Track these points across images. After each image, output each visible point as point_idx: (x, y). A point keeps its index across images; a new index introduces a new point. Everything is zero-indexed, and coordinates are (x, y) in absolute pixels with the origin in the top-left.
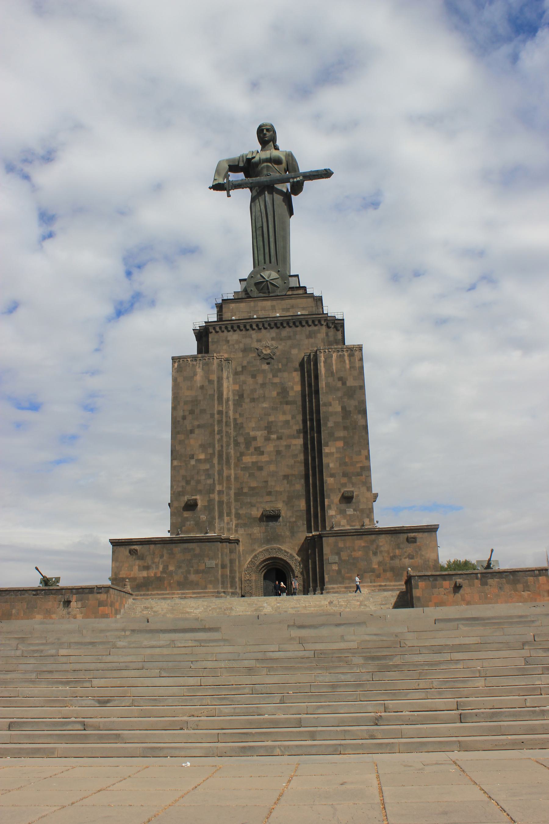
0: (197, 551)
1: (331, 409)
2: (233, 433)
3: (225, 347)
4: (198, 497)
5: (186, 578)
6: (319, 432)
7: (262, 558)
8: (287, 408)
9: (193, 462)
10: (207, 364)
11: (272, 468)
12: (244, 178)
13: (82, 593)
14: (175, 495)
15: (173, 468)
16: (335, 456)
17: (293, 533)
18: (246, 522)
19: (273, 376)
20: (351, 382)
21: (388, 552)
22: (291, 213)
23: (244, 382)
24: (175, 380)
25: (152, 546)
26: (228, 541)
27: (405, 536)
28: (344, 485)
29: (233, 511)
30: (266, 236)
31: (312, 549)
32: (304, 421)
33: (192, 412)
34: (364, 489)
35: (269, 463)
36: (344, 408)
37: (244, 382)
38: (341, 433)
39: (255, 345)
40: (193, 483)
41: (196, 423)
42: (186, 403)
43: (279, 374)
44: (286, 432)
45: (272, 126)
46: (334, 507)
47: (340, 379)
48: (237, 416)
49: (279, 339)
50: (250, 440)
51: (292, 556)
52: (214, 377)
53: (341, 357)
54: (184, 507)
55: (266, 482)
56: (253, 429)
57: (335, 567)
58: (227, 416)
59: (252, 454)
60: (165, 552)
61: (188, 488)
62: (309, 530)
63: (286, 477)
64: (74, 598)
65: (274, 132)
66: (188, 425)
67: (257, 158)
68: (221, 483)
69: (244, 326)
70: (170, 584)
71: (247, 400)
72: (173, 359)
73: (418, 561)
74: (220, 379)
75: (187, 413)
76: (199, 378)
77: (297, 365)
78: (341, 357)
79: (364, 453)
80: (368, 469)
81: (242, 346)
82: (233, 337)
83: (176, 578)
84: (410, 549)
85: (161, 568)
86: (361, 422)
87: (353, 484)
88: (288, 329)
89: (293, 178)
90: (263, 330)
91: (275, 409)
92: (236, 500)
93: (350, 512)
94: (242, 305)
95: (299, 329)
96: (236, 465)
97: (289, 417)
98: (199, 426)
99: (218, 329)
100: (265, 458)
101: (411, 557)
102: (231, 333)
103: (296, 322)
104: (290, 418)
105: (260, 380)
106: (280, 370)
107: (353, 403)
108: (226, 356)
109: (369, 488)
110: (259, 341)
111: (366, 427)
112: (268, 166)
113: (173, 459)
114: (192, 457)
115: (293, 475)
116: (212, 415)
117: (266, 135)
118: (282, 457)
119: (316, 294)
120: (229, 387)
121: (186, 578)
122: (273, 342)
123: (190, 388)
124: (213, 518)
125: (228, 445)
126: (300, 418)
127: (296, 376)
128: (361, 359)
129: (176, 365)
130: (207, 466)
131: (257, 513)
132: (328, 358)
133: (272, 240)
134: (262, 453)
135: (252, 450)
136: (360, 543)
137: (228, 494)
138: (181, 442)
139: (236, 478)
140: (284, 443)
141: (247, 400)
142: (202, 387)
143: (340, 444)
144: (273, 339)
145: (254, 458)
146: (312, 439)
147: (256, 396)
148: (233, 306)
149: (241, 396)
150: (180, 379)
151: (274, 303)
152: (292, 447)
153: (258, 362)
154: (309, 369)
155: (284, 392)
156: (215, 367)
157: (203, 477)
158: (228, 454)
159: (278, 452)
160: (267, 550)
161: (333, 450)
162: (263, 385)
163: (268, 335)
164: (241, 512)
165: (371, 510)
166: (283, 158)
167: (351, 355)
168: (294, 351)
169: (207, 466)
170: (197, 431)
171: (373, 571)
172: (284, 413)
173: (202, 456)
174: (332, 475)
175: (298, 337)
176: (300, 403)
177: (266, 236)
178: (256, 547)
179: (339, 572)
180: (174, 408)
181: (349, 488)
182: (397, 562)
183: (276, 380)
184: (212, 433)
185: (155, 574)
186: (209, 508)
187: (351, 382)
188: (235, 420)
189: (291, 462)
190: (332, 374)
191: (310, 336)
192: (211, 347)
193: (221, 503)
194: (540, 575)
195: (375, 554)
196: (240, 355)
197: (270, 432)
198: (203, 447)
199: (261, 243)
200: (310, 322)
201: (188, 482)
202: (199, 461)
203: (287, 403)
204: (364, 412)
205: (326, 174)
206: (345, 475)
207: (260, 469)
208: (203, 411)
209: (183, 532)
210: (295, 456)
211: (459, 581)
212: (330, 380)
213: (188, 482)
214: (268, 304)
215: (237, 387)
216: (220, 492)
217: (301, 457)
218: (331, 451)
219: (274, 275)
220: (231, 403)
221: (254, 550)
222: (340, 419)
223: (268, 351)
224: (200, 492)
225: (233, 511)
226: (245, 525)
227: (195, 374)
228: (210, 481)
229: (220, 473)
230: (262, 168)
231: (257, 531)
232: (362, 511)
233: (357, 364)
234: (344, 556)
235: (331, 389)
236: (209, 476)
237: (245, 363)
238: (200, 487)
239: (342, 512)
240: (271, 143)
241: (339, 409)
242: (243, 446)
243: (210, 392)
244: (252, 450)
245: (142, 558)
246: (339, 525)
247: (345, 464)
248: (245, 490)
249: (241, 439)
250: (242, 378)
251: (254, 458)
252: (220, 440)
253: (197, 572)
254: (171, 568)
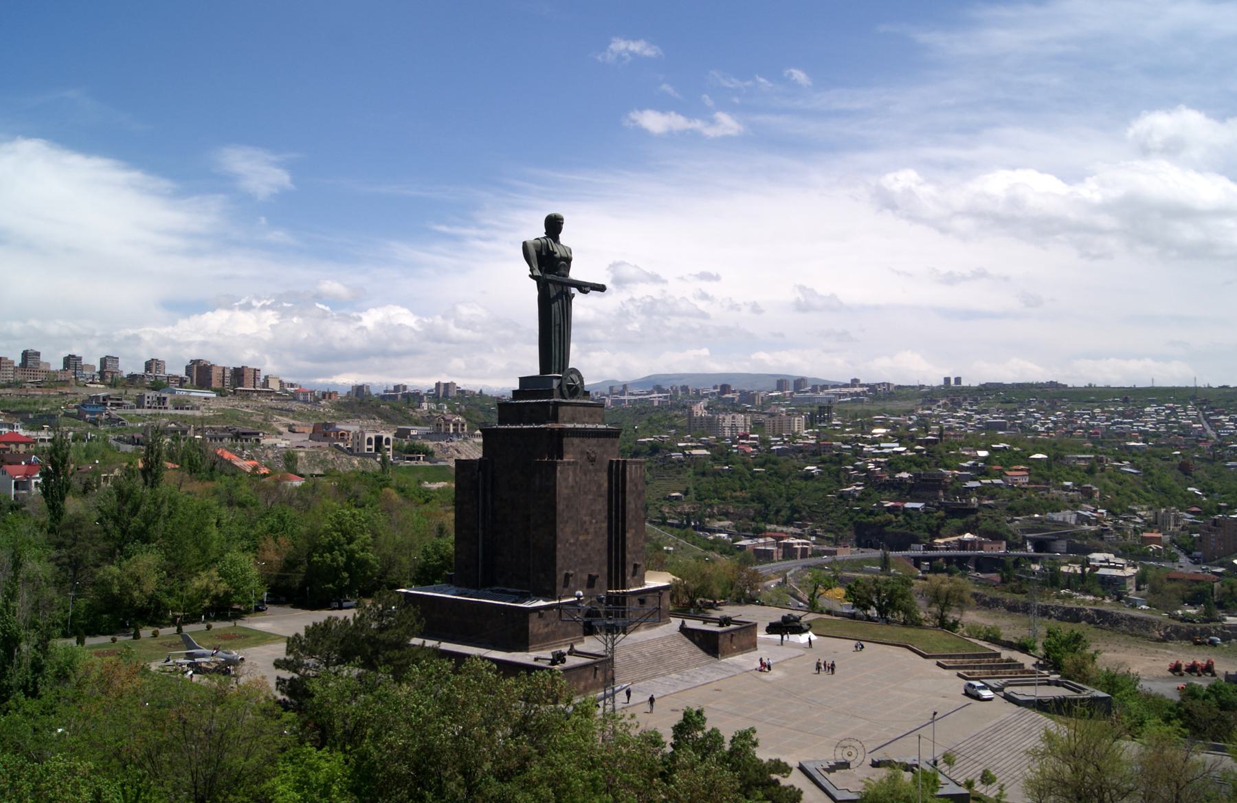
8: (600, 499)
32: (610, 510)
38: (634, 524)
76: (570, 479)
77: (606, 466)
82: (576, 441)
100: (590, 537)
127: (605, 476)
155: (600, 486)
190: (632, 481)
205: (601, 288)
207: (587, 545)
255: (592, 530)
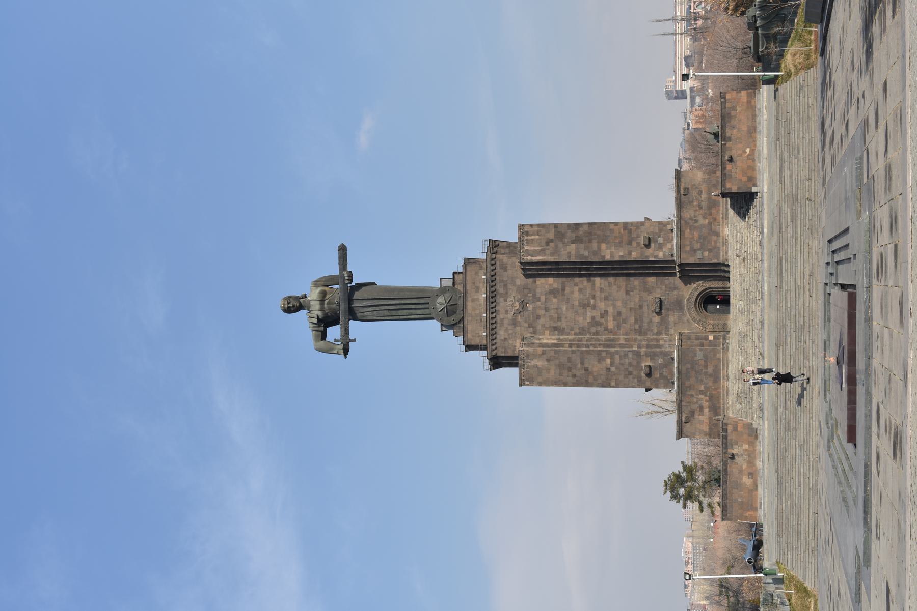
0: (689, 366)
1: (573, 253)
2: (588, 336)
3: (511, 342)
4: (643, 365)
5: (711, 376)
6: (592, 263)
7: (694, 314)
8: (568, 290)
9: (613, 369)
10: (528, 356)
11: (619, 304)
12: (338, 326)
13: (726, 444)
14: (640, 384)
15: (617, 386)
16: (613, 250)
17: (675, 288)
18: (664, 326)
19: (539, 300)
20: (551, 235)
21: (696, 211)
22: (374, 284)
23: (543, 326)
24: (540, 384)
25: (683, 404)
26: (680, 341)
27: (683, 198)
28: (638, 244)
29: (655, 337)
30: (398, 307)
31: (689, 273)
32: (580, 276)
33: (570, 369)
34: (643, 228)
35: (614, 306)
36: (573, 242)
37: (543, 326)
38: (595, 245)
39: (510, 316)
40: (631, 369)
41: (579, 366)
42: (561, 375)
43: (538, 295)
44: (588, 291)
45: (285, 299)
46: (656, 253)
47: (547, 243)
48: (573, 332)
49: (506, 295)
50: (595, 322)
51: (695, 289)
52: (540, 350)
53: (528, 242)
54: (650, 378)
55: (631, 309)
56: (585, 319)
57: (706, 254)
58: (573, 340)
59: (607, 321)
60: (689, 393)
61: (635, 373)
62: (674, 274)
63: (627, 292)
64: (730, 451)
65: (290, 297)
66: (579, 373)
67: (320, 314)
68: (631, 346)
69: (493, 327)
70: (716, 389)
71: (559, 324)
72: (521, 385)
73: (704, 187)
74: (541, 345)
75: (570, 374)
77: (530, 280)
78: (528, 242)
79: (612, 226)
80: (626, 225)
81: (510, 327)
82: (501, 334)
83: (710, 384)
84: (694, 193)
85: (702, 397)
86: (586, 228)
87: (638, 236)
88: (498, 287)
89: (344, 280)
90: (497, 308)
91: (568, 300)
92: (645, 334)
93: (661, 240)
94: (469, 327)
95: (498, 278)
96: (615, 334)
97: (576, 288)
98: (582, 363)
99: (494, 347)
100: (611, 310)
101: (700, 193)
102: (498, 337)
103: (492, 280)
104: (577, 288)
105: (541, 312)
106: (534, 295)
107: (570, 235)
108: (518, 341)
109: (642, 224)
110: (507, 312)
111: (590, 224)
112: (328, 303)
113: (609, 385)
114: (608, 369)
115: (626, 286)
116: (573, 352)
117: (294, 306)
118: (611, 294)
119: (462, 262)
120: (548, 339)
121: (711, 376)
122: (509, 300)
123: (548, 370)
124: (661, 352)
125: (599, 340)
126: (577, 280)
127: (540, 281)
128: (531, 226)
129: (527, 383)
130: (617, 356)
131: (657, 319)
132: (528, 253)
133: (403, 302)
134: (606, 312)
135: (602, 320)
136: (687, 232)
137: (641, 341)
138: (595, 379)
139: (626, 334)
140: (598, 294)
141: (559, 324)
142: (548, 360)
143: (604, 246)
144: (506, 300)
145: (610, 319)
146: (596, 269)
147: (556, 316)
148: (469, 336)
149: (555, 328)
150: (540, 379)
151: (469, 299)
152: (602, 286)
153: (526, 313)
154: (533, 270)
155: (553, 292)
156: (531, 350)
157: (627, 360)
158: (606, 340)
159: (606, 298)
160: (689, 310)
161: (608, 252)
162: (547, 309)
163: (502, 305)
164: (655, 331)
165: (660, 223)
166: (319, 289)
167: (527, 234)
168: (518, 282)
169: (617, 356)
170: (586, 365)
171: (710, 223)
172: (572, 292)
173: (608, 361)
174: (630, 253)
175: (505, 279)
176: (564, 279)
177: (398, 307)
178: (685, 319)
179: (710, 251)
180: (565, 385)
181: (642, 241)
182: (704, 204)
183: (543, 298)
184: (588, 352)
185: (706, 401)
186: (652, 356)
187: (551, 235)
188: (576, 334)
189: (615, 287)
191: (505, 268)
192: (510, 354)
193: (648, 346)
194: (725, 98)
195: (696, 221)
196: (518, 329)
197: (589, 305)
198: (600, 360)
199: (405, 312)
200: (493, 267)
201: (630, 373)
202: (612, 364)
203: (563, 289)
204: (577, 225)
205: (343, 250)
206: (630, 243)
207: (619, 314)
208: (569, 360)
209: (672, 378)
210: (610, 285)
211: (727, 158)
212: (548, 252)
213: (630, 373)
214: (470, 305)
215: (547, 332)
216: (639, 347)
217: (611, 279)
218: (610, 253)
219: (441, 299)
220: (561, 337)
221: (688, 320)
222: (582, 246)
223: (517, 304)
224: (639, 363)
225: (655, 337)
226: (667, 328)
227: (536, 366)
228: (630, 355)
229: (622, 346)
230: (330, 309)
231: (672, 319)
232: (661, 230)
233: (536, 229)
234: (697, 246)
235: (556, 252)
236: (626, 355)
237: (526, 325)
238: (635, 363)
239: (660, 247)
240: (301, 300)
241: (574, 246)
242: (599, 328)
243: (552, 353)
244: (602, 320)
245: (692, 413)
246: (672, 249)
247: (621, 242)
248: (637, 327)
249: (593, 330)
250: (539, 327)
251: (610, 319)
252: (594, 346)
253: (706, 366)
254: (702, 388)
255: (602, 305)
